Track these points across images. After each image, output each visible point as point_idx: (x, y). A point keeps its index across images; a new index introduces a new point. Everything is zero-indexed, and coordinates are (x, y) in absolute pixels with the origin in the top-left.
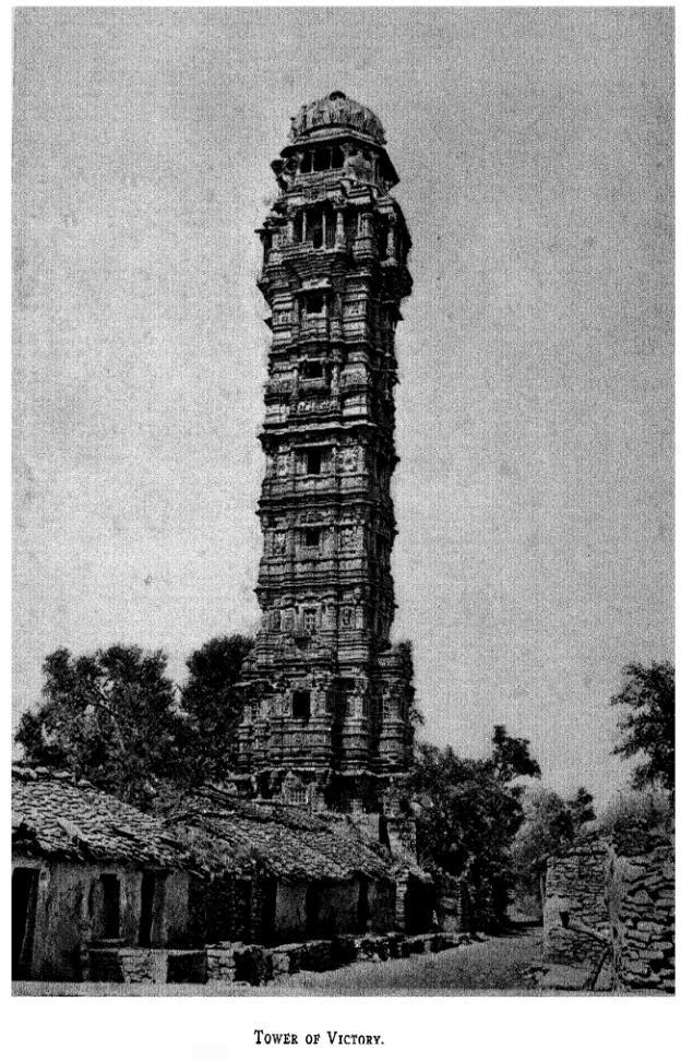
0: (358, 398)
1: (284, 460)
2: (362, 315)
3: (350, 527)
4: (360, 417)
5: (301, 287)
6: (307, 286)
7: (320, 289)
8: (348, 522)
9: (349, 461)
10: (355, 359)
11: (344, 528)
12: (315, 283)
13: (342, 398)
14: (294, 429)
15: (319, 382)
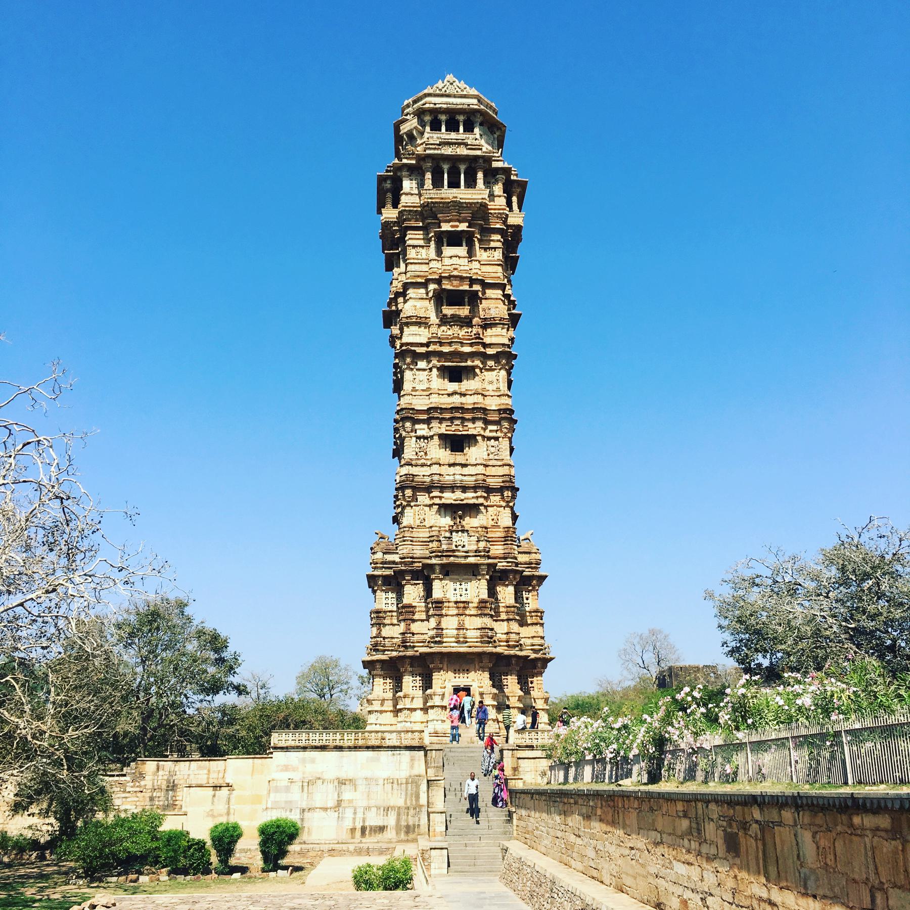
0: (499, 329)
1: (423, 375)
2: (499, 260)
3: (496, 439)
4: (503, 345)
5: (440, 227)
6: (446, 227)
7: (463, 231)
8: (494, 434)
9: (491, 383)
10: (493, 296)
11: (489, 439)
12: (457, 226)
13: (485, 327)
14: (436, 348)
15: (464, 311)
